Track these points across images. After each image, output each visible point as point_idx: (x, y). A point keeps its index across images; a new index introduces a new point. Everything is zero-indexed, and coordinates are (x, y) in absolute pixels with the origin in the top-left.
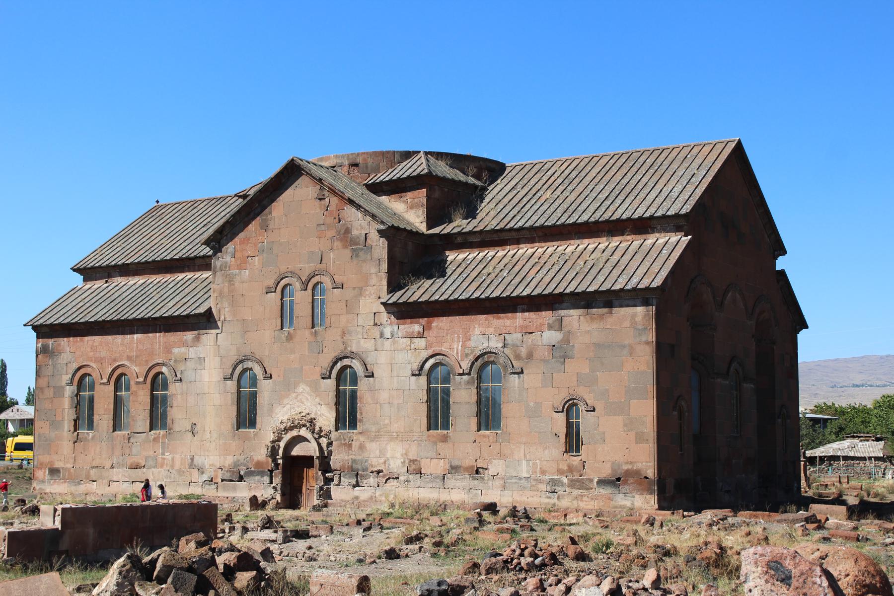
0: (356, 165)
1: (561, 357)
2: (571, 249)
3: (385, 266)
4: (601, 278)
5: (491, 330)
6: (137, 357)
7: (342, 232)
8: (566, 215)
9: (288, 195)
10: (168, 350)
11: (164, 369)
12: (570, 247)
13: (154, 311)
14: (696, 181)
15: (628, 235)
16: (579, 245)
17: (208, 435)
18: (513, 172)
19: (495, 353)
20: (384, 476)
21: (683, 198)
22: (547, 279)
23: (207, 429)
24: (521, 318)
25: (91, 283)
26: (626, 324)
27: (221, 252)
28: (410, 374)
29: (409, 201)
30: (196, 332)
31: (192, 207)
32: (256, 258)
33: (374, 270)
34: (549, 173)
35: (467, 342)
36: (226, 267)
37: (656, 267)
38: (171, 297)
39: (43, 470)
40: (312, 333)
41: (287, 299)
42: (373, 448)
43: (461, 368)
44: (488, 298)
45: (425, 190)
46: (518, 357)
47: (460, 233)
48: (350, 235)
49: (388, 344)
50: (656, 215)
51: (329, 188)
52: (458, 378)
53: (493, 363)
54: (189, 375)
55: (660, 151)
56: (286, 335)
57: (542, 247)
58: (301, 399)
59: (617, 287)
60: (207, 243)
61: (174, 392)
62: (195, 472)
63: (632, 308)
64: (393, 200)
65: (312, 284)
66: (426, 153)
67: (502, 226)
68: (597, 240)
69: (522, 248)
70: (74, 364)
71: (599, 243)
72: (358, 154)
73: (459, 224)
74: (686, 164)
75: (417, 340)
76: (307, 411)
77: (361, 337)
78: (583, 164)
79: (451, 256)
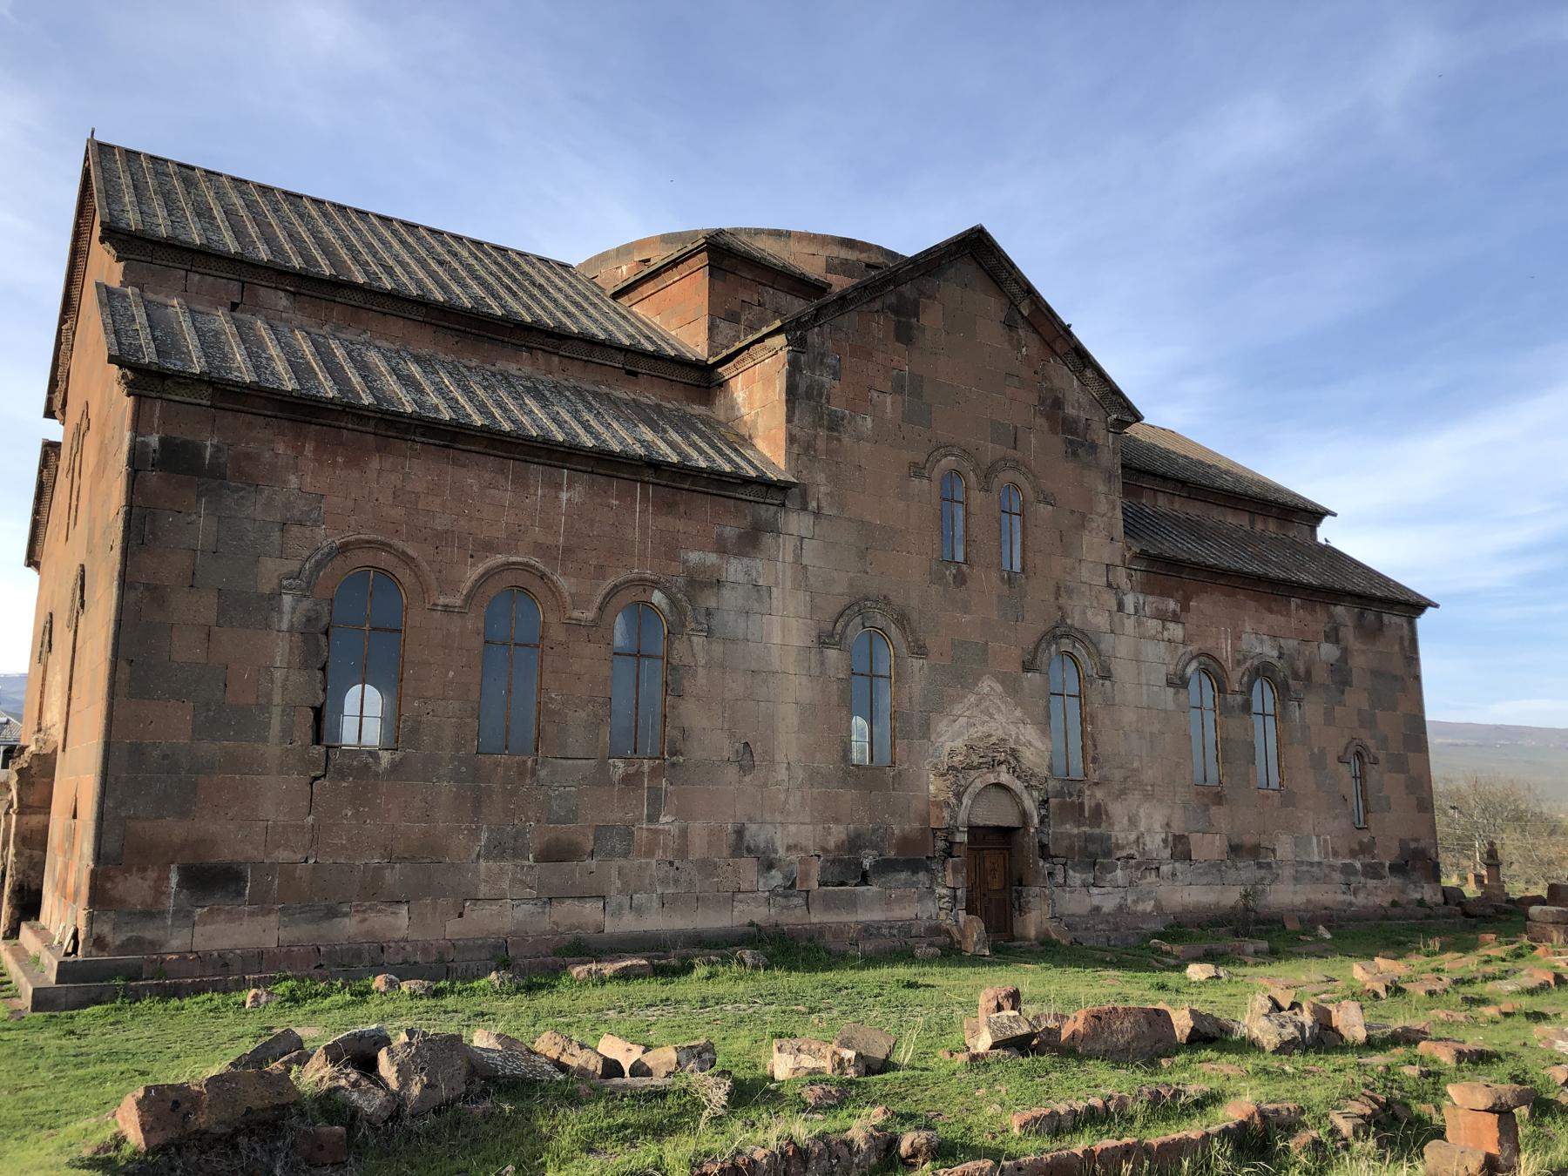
6: (568, 550)
7: (1049, 401)
10: (671, 551)
11: (657, 597)
17: (782, 774)
20: (1138, 866)
23: (780, 757)
26: (1397, 648)
28: (1164, 682)
32: (889, 399)
33: (1102, 488)
36: (820, 394)
39: (152, 874)
42: (1117, 810)
46: (1296, 676)
48: (1061, 412)
56: (954, 571)
58: (987, 708)
61: (685, 661)
62: (748, 865)
70: (321, 531)
75: (1171, 626)
76: (1000, 733)
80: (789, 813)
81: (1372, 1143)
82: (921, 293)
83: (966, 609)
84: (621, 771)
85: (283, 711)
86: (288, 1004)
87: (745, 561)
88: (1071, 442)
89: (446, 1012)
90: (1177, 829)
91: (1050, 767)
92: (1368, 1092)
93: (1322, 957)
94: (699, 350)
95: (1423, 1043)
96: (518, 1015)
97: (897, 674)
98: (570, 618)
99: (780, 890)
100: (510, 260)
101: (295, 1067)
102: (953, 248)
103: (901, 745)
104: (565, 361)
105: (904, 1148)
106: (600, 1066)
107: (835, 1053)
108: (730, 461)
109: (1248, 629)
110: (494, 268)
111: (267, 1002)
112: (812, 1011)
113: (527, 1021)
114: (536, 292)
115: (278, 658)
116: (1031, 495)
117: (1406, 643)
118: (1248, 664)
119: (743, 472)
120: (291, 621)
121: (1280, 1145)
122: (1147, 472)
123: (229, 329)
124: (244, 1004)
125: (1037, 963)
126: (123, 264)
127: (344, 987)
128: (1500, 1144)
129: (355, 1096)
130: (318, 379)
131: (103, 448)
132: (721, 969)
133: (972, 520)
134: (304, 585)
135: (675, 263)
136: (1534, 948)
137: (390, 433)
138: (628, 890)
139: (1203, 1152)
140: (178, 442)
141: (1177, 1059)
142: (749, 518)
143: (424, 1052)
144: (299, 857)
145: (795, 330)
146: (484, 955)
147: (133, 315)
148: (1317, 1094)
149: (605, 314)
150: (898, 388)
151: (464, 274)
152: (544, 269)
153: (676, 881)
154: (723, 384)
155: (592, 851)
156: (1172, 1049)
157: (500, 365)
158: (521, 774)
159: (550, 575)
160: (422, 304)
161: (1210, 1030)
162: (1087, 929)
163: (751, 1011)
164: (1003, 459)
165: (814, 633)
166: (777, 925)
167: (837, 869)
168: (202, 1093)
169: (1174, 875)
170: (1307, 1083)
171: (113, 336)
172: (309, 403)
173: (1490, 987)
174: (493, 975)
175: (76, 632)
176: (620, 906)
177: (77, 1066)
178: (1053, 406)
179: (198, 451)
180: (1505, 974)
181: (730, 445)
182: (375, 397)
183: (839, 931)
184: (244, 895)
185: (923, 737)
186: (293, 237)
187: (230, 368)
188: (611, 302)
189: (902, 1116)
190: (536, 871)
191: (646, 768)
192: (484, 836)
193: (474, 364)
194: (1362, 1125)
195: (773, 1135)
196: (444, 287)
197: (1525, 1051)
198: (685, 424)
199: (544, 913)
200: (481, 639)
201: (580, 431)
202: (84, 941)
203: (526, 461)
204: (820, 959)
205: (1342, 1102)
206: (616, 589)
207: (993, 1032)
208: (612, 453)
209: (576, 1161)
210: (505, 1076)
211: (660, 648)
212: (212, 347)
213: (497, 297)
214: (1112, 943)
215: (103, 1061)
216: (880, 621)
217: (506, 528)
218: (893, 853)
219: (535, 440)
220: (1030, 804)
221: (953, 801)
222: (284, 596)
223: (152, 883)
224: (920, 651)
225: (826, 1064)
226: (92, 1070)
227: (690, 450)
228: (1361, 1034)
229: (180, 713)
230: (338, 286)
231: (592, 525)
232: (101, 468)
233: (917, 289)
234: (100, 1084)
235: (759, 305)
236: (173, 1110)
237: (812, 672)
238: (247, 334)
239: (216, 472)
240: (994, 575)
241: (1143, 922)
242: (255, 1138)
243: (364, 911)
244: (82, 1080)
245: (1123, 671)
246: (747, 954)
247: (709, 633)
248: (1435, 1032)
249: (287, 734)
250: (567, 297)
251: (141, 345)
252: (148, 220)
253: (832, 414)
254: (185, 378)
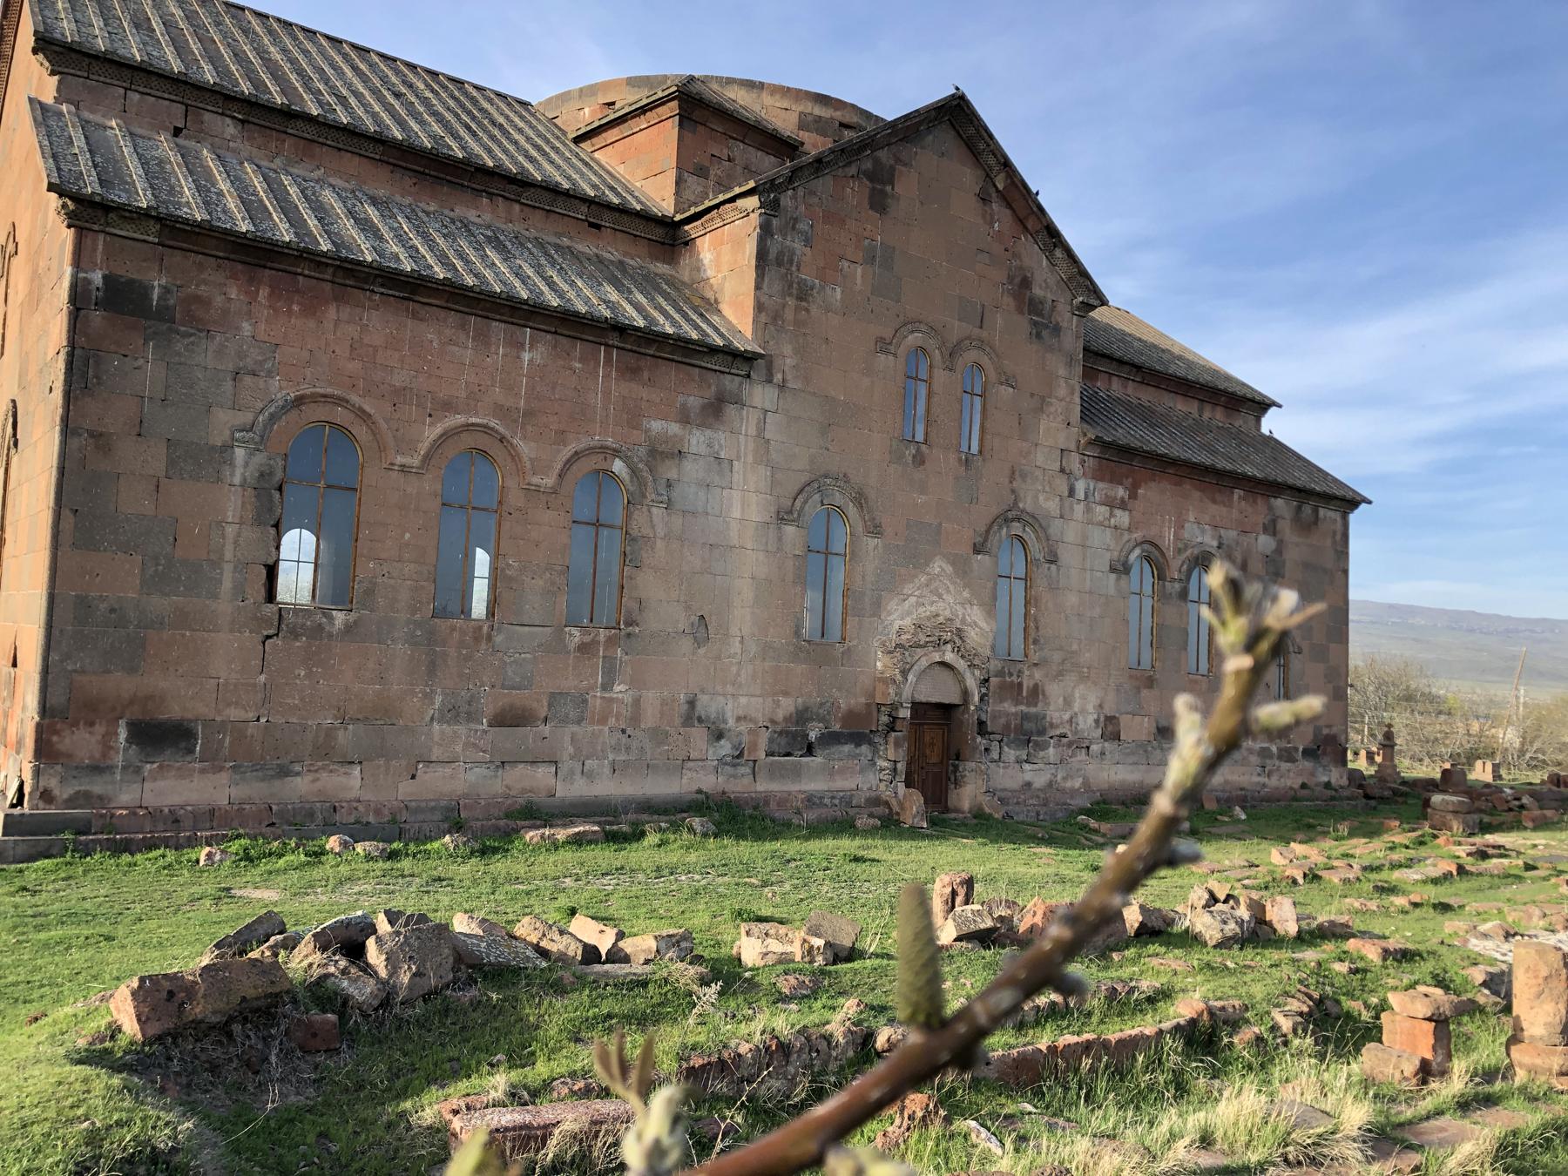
6: (529, 414)
7: (1017, 280)
10: (634, 417)
11: (618, 466)
17: (736, 647)
20: (1070, 745)
23: (734, 630)
26: (1329, 542)
33: (1062, 372)
36: (791, 262)
39: (100, 729)
40: (960, 459)
42: (1054, 690)
54: (688, 493)
61: (646, 531)
62: (699, 735)
70: (276, 382)
75: (1118, 512)
76: (947, 613)
80: (740, 685)
81: (1309, 1040)
82: (898, 160)
83: (923, 491)
84: (576, 639)
85: (235, 567)
86: (242, 864)
87: (708, 432)
88: (1035, 324)
89: (403, 876)
90: (1108, 711)
91: (993, 648)
92: (1303, 989)
93: (1240, 839)
94: (664, 204)
95: (1352, 940)
96: (476, 883)
97: (853, 553)
98: (529, 484)
99: (729, 759)
100: (466, 94)
101: (282, 953)
102: (933, 113)
103: (852, 622)
104: (526, 209)
105: (881, 1042)
106: (580, 952)
107: (805, 941)
108: (697, 327)
110: (452, 103)
111: (221, 861)
112: (765, 884)
113: (485, 888)
114: (496, 132)
115: (230, 514)
116: (993, 376)
117: (1338, 537)
118: (1188, 552)
119: (709, 341)
120: (243, 474)
121: (1226, 1040)
122: (1104, 356)
123: (174, 157)
124: (198, 861)
125: (974, 838)
126: (56, 78)
127: (298, 847)
128: (1434, 1049)
129: (345, 984)
130: (272, 220)
131: (35, 277)
132: (672, 837)
133: (935, 399)
134: (257, 439)
135: (643, 110)
136: (1435, 837)
137: (348, 282)
138: (580, 757)
139: (1156, 1047)
140: (123, 280)
141: (1126, 953)
142: (713, 388)
143: (412, 941)
144: (251, 715)
145: (769, 193)
146: (438, 816)
147: (70, 137)
148: (1258, 991)
149: (567, 160)
150: (870, 259)
151: (422, 109)
152: (503, 106)
153: (628, 749)
154: (688, 243)
155: (546, 718)
156: (1124, 943)
157: (459, 211)
158: (477, 639)
159: (509, 437)
160: (380, 141)
161: (1156, 923)
162: (1018, 803)
163: (704, 882)
164: (968, 338)
165: (773, 509)
166: (724, 793)
167: (783, 741)
168: (197, 983)
169: (1103, 754)
170: (1247, 978)
171: (51, 160)
172: (263, 245)
173: (1396, 875)
174: (447, 838)
175: (7, 470)
176: (572, 772)
177: (39, 928)
178: (1022, 284)
179: (145, 291)
180: (1409, 863)
181: (695, 309)
182: (333, 243)
183: (782, 802)
184: (191, 751)
185: (873, 615)
186: (238, 56)
187: (179, 203)
188: (572, 146)
189: (872, 1008)
190: (490, 737)
191: (602, 638)
192: (438, 699)
193: (432, 209)
194: (1301, 1023)
195: (757, 1026)
196: (402, 124)
197: (1443, 950)
198: (649, 284)
199: (496, 777)
200: (439, 501)
201: (545, 289)
202: (30, 794)
203: (487, 318)
204: (765, 828)
205: (1281, 1000)
206: (577, 455)
207: (958, 926)
208: (577, 314)
209: (565, 1051)
210: (490, 963)
211: (618, 518)
212: (158, 178)
213: (456, 137)
214: (1041, 817)
215: (63, 923)
216: (838, 499)
217: (467, 386)
218: (838, 726)
219: (499, 296)
220: (971, 683)
221: (899, 678)
222: (236, 449)
223: (100, 737)
224: (875, 530)
225: (796, 950)
226: (55, 933)
227: (656, 314)
228: (1292, 929)
229: (127, 566)
230: (290, 116)
231: (554, 388)
232: (34, 300)
233: (894, 155)
234: (66, 949)
235: (729, 160)
236: (168, 1000)
237: (770, 548)
238: (194, 164)
239: (164, 315)
240: (952, 457)
241: (1072, 798)
242: (249, 1026)
243: (316, 771)
244: (46, 945)
245: (1068, 555)
246: (697, 822)
247: (669, 505)
248: (1358, 924)
249: (239, 591)
250: (528, 139)
251: (81, 173)
252: (84, 30)
253: (801, 283)
254: (130, 211)
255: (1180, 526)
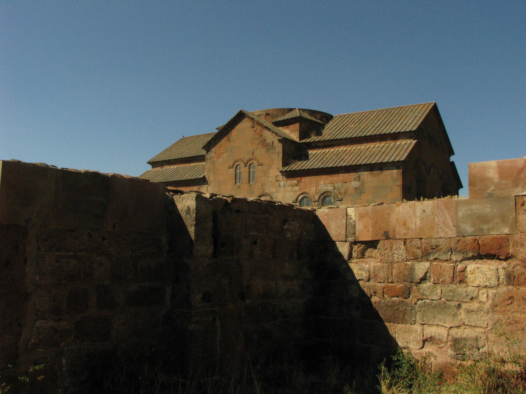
0: (268, 114)
1: (360, 193)
2: (363, 147)
3: (281, 155)
4: (377, 158)
5: (328, 182)
7: (263, 141)
8: (361, 133)
9: (239, 126)
12: (363, 147)
13: (181, 178)
14: (417, 118)
15: (388, 141)
16: (366, 146)
18: (337, 118)
19: (330, 192)
21: (412, 125)
22: (353, 159)
24: (341, 176)
25: (155, 168)
27: (210, 152)
29: (291, 129)
30: (199, 186)
31: (198, 138)
33: (276, 157)
34: (352, 118)
35: (317, 188)
36: (212, 158)
37: (402, 153)
38: (188, 172)
41: (238, 171)
43: (315, 199)
44: (327, 168)
45: (298, 124)
46: (340, 193)
47: (314, 142)
49: (282, 189)
50: (401, 131)
51: (257, 122)
52: (313, 203)
53: (329, 196)
55: (401, 108)
56: (237, 186)
57: (350, 147)
59: (385, 161)
60: (203, 148)
63: (391, 170)
64: (284, 129)
65: (248, 164)
66: (299, 109)
67: (332, 138)
68: (375, 144)
69: (341, 148)
71: (376, 145)
72: (269, 110)
73: (314, 138)
74: (413, 112)
75: (295, 187)
77: (270, 186)
78: (367, 114)
79: (310, 152)
88: (267, 149)
109: (322, 183)
255: (317, 185)
